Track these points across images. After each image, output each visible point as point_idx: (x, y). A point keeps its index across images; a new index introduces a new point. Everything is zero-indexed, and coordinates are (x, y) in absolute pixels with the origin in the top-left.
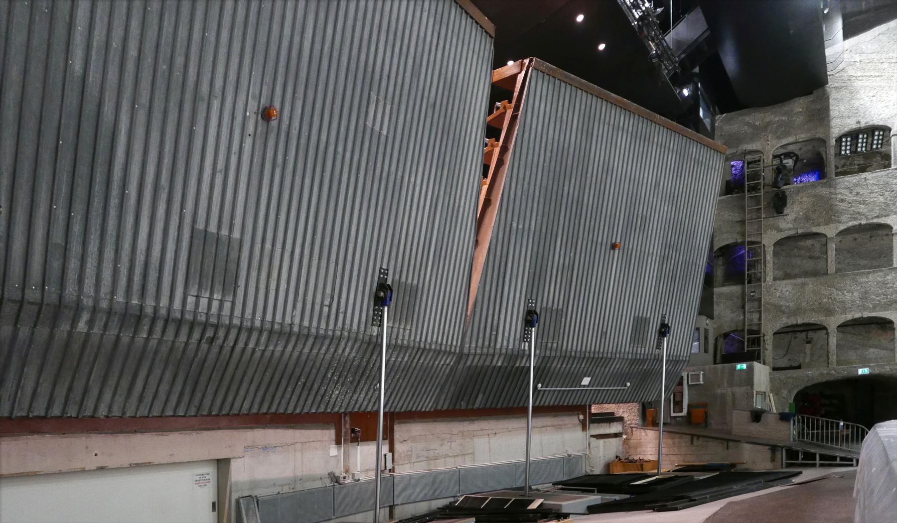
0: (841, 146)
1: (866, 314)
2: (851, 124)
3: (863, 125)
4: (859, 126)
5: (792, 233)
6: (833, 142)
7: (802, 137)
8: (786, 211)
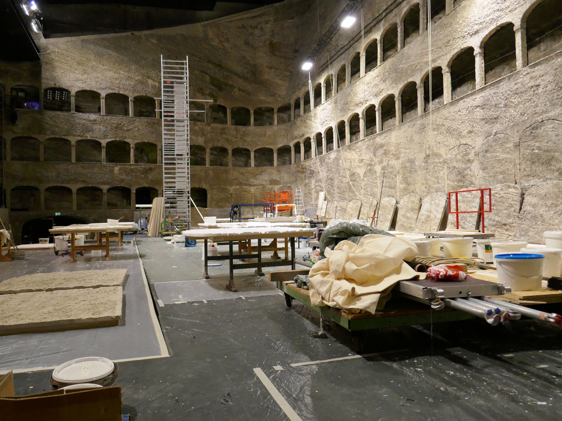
0: (47, 94)
1: (59, 185)
2: (51, 84)
3: (57, 86)
4: (55, 86)
5: (21, 135)
6: (43, 91)
7: (27, 84)
8: (18, 122)
